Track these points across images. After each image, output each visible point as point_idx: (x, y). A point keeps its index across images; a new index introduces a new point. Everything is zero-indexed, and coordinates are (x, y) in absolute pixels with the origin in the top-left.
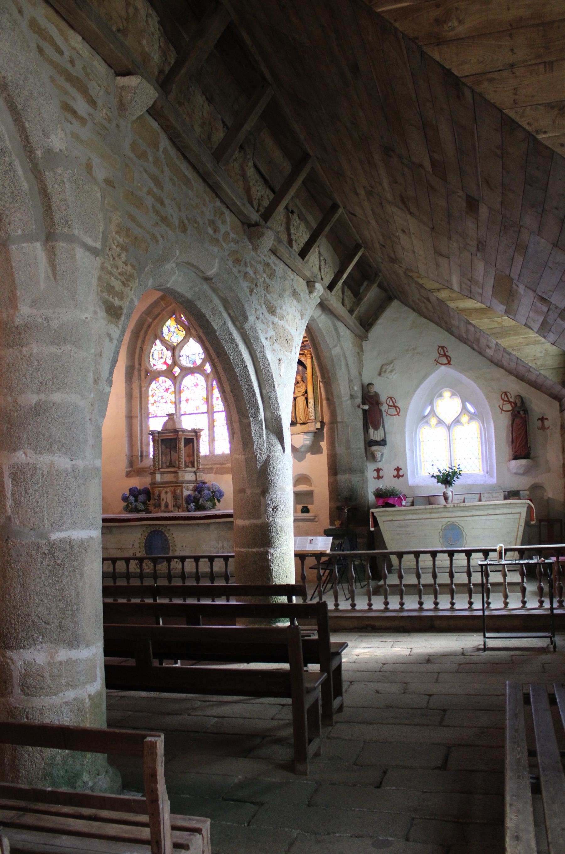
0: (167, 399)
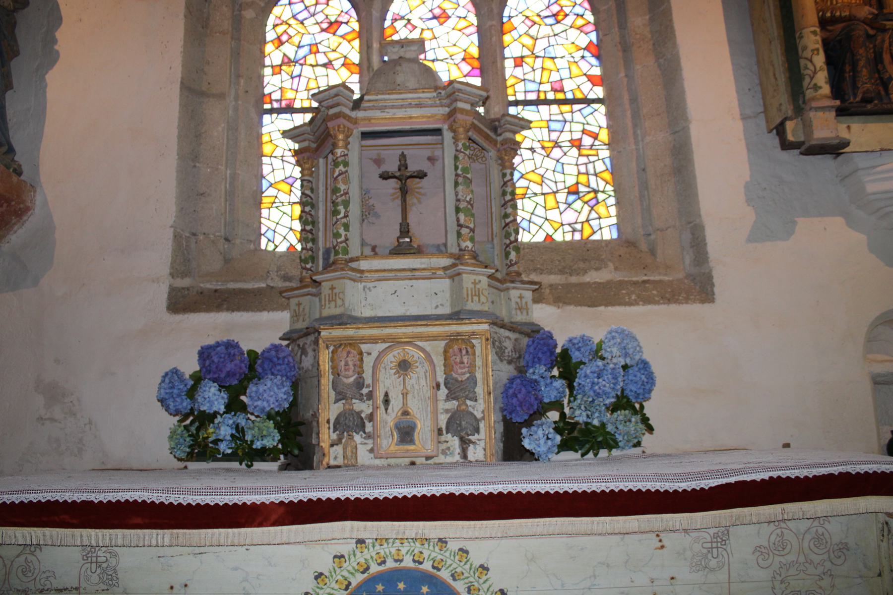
0: (332, 56)
